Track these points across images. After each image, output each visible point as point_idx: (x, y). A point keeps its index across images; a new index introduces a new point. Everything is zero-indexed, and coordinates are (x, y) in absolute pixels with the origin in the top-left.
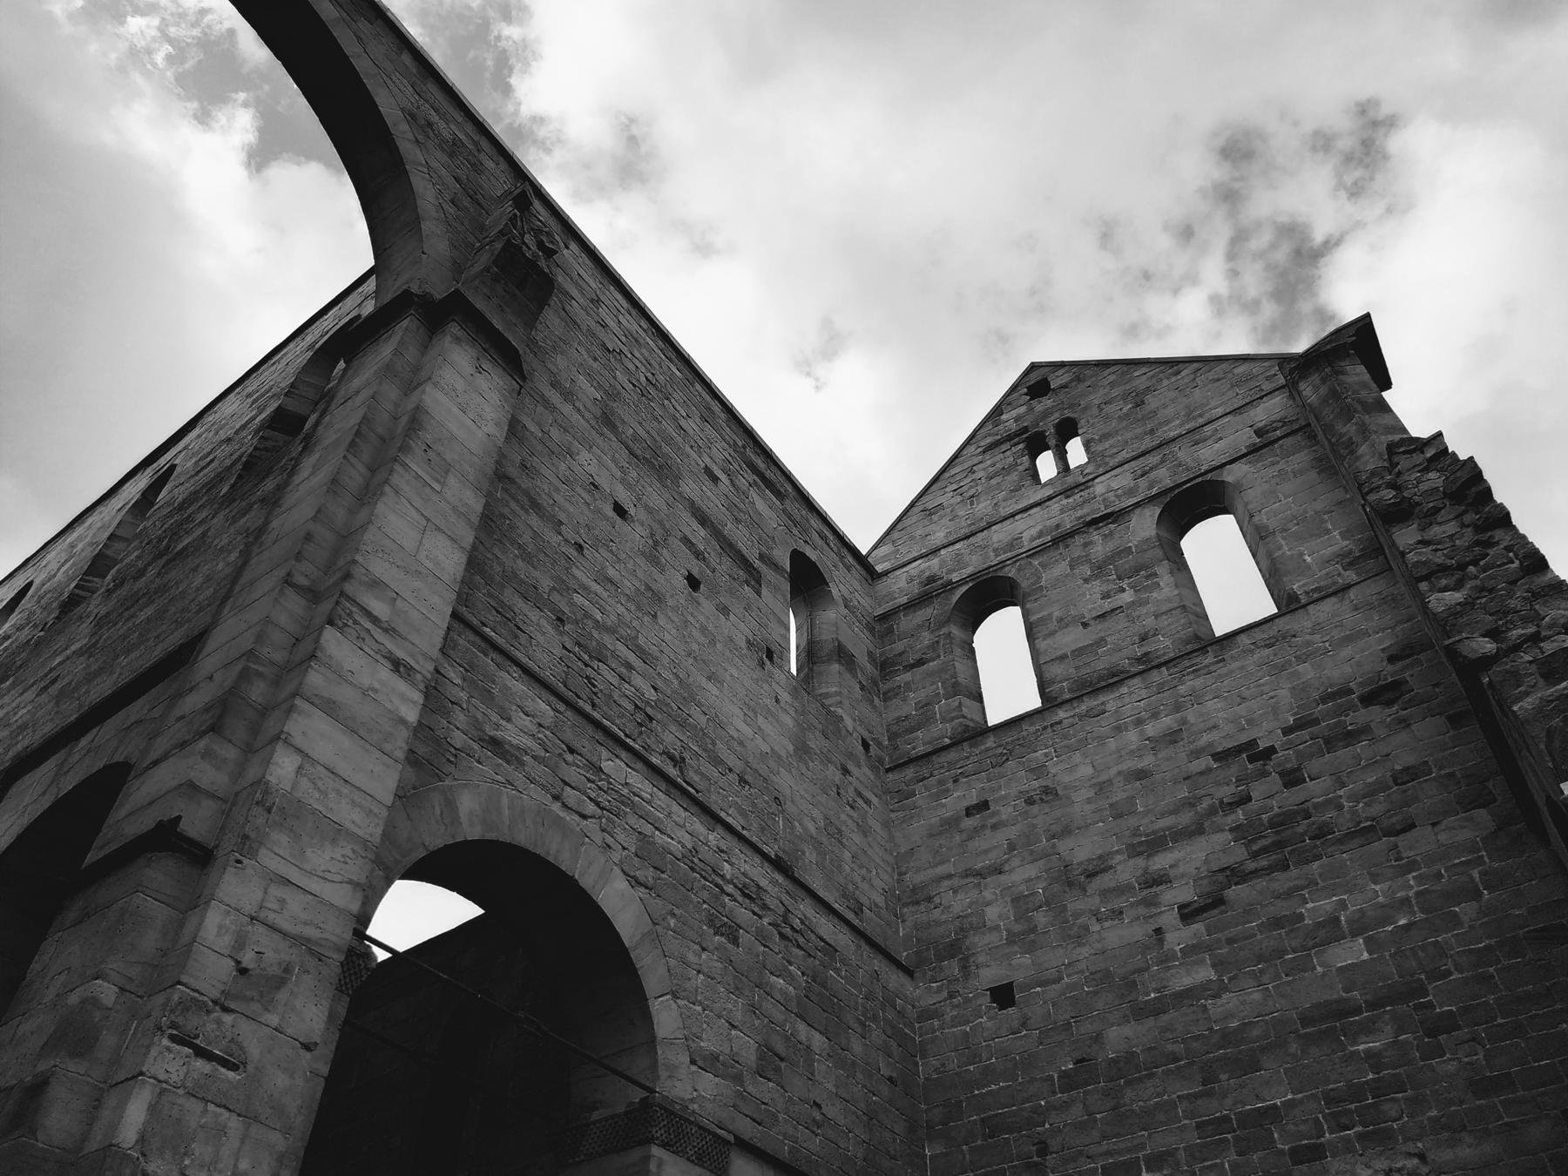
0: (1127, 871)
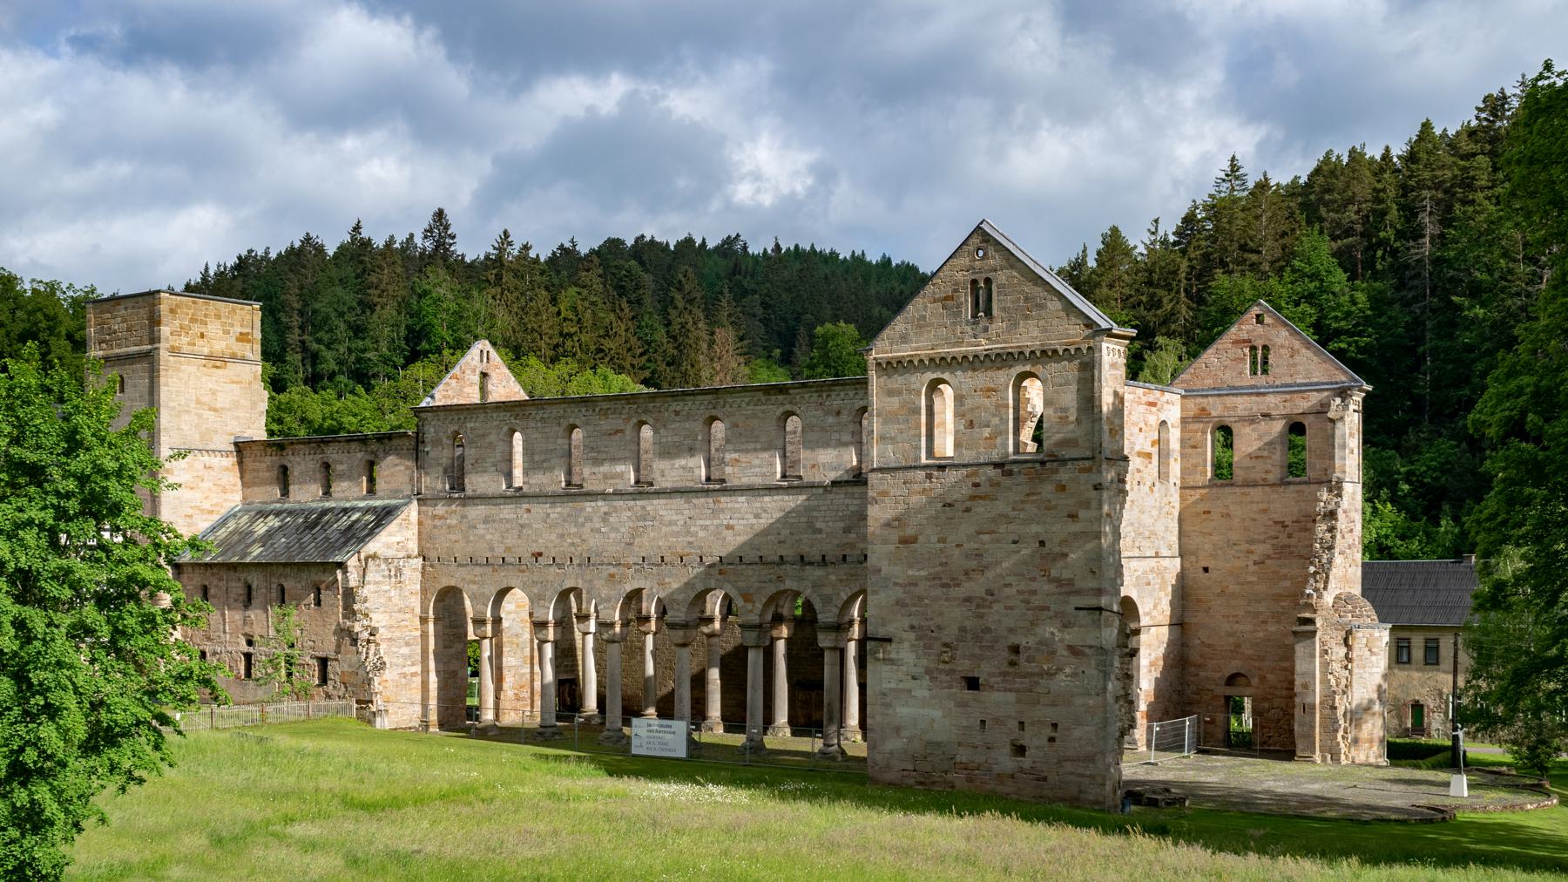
0: (1245, 547)
